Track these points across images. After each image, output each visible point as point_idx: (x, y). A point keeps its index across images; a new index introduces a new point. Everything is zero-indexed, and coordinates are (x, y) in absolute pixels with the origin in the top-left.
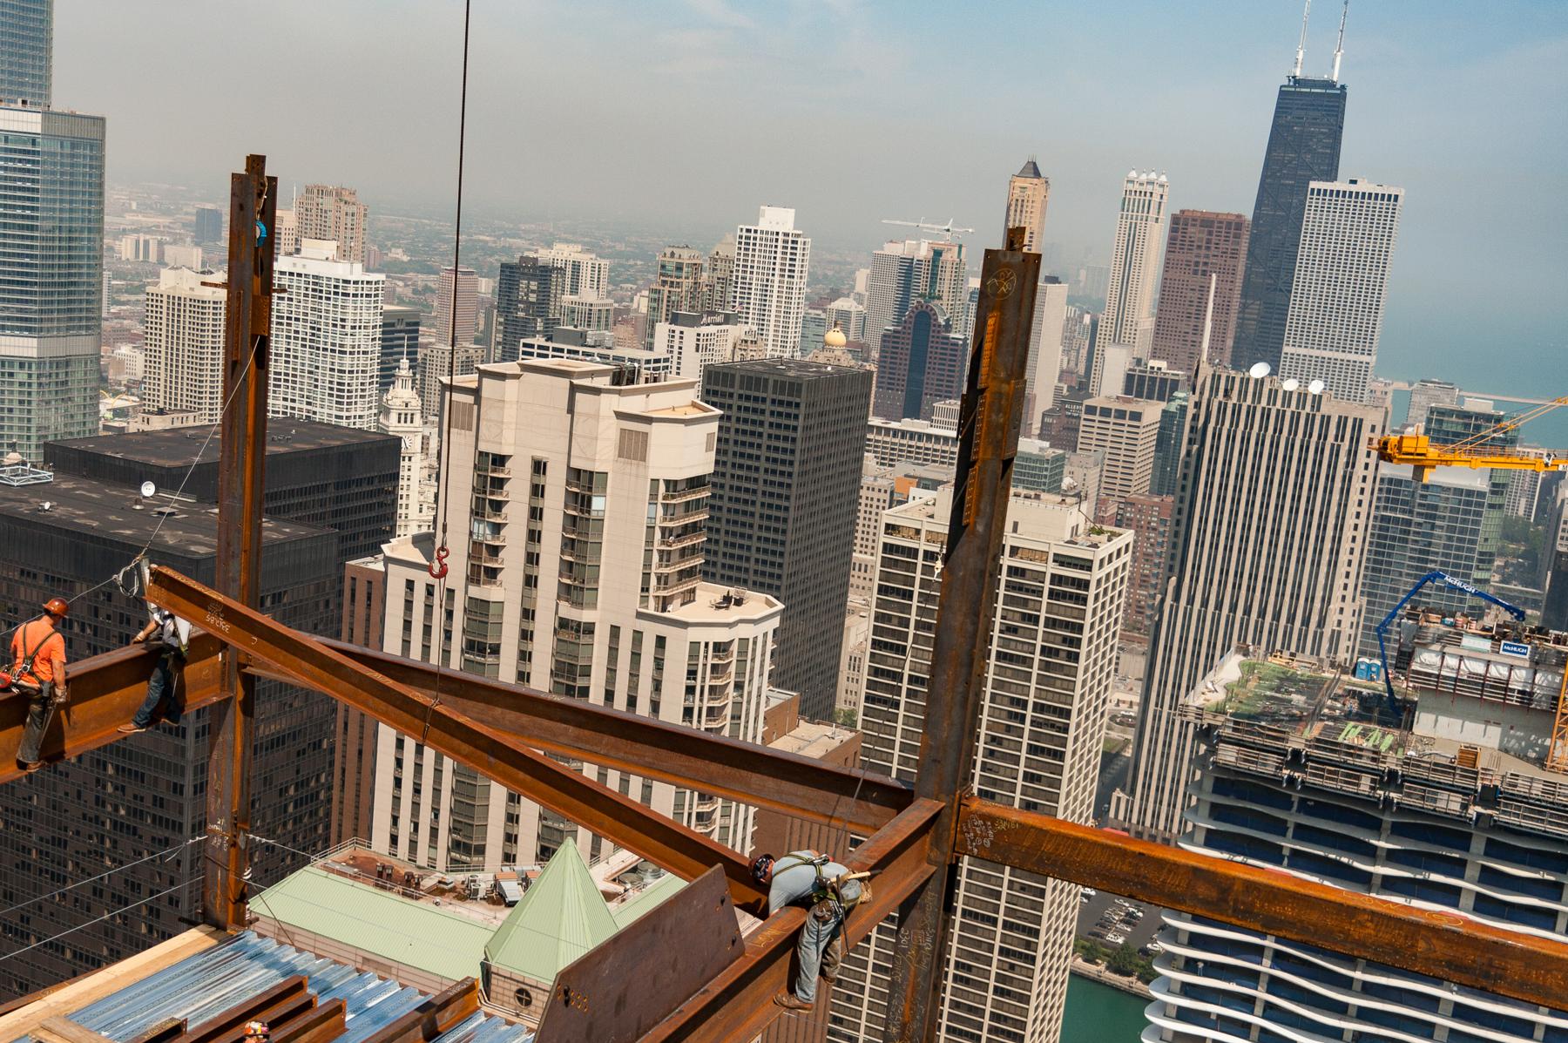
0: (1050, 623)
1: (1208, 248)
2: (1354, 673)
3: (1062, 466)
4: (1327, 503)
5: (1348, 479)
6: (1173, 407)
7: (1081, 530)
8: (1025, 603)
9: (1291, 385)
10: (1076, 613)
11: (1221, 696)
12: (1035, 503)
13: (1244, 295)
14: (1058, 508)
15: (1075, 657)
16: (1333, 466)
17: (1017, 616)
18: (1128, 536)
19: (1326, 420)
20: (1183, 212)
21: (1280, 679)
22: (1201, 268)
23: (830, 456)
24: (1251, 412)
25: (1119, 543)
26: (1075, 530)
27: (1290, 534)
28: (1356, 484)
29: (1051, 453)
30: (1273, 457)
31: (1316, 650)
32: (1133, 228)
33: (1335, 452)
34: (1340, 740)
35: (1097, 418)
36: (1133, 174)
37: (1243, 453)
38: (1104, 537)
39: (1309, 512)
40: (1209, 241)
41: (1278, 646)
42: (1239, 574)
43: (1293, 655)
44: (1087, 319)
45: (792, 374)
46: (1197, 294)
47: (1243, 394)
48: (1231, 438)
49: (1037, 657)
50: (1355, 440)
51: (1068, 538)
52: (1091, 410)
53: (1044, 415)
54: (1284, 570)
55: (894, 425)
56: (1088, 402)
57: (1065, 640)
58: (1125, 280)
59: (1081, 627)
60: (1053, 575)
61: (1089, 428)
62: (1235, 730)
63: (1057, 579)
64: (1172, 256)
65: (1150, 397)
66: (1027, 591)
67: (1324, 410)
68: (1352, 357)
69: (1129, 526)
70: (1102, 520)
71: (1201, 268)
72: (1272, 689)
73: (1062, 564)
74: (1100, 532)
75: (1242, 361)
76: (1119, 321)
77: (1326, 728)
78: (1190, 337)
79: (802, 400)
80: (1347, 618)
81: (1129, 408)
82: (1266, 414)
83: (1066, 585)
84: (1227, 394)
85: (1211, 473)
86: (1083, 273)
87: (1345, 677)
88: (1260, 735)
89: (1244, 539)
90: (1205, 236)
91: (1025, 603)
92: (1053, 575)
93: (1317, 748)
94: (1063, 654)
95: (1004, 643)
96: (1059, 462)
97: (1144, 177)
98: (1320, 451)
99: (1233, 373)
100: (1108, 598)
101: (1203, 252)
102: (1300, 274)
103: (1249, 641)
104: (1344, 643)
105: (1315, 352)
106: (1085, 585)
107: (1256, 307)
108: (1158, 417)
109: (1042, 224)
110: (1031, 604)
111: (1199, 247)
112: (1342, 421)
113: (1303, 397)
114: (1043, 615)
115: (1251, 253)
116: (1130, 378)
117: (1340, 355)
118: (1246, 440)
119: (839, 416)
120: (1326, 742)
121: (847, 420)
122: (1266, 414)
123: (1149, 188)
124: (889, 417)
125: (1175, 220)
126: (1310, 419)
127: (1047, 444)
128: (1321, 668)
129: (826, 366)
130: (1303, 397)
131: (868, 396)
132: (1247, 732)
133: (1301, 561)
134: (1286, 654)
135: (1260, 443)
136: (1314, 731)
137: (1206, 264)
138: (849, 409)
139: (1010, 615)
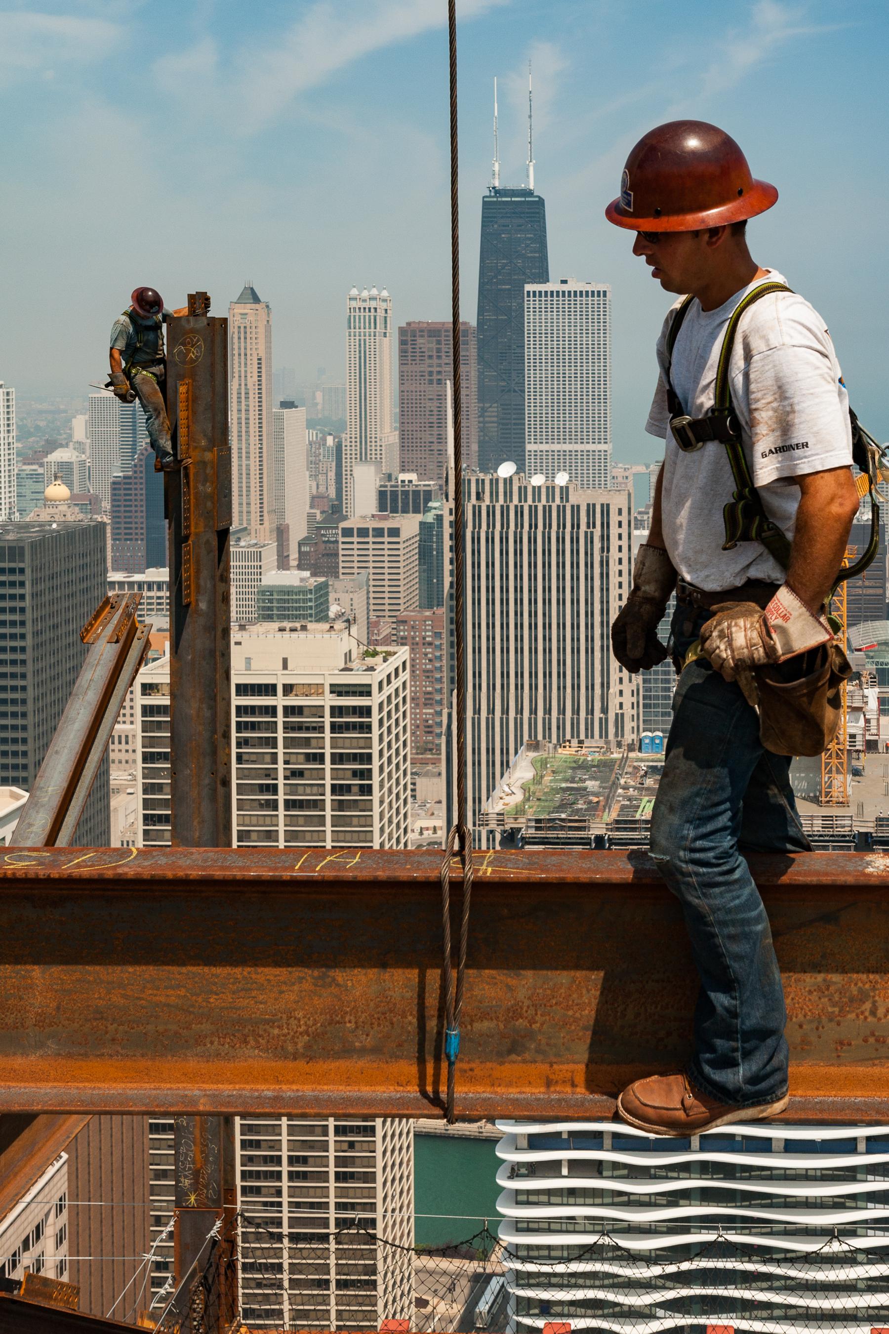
0: (337, 758)
1: (439, 357)
2: (640, 750)
3: (327, 594)
4: (590, 590)
5: (605, 563)
6: (430, 518)
7: (354, 655)
8: (307, 742)
9: (538, 480)
10: (362, 743)
11: (519, 797)
12: (302, 635)
13: (481, 399)
14: (327, 636)
15: (367, 790)
16: (589, 554)
17: (301, 758)
18: (403, 653)
19: (576, 509)
20: (409, 324)
21: (573, 768)
22: (435, 377)
23: (67, 622)
24: (505, 511)
25: (395, 662)
26: (348, 656)
27: (561, 626)
28: (614, 568)
29: (313, 582)
30: (533, 553)
31: (604, 733)
32: (362, 344)
33: (589, 539)
34: (638, 817)
35: (355, 539)
36: (354, 292)
37: (504, 553)
38: (379, 659)
39: (575, 602)
40: (439, 350)
41: (568, 737)
42: (519, 675)
43: (581, 742)
44: (330, 441)
45: (11, 537)
46: (436, 403)
47: (494, 495)
48: (490, 540)
49: (328, 797)
50: (606, 525)
51: (342, 666)
52: (347, 532)
53: (300, 545)
54: (562, 663)
55: (137, 577)
56: (343, 525)
57: (355, 774)
58: (363, 398)
59: (369, 756)
60: (332, 708)
61: (349, 551)
62: (537, 829)
63: (337, 711)
64: (405, 368)
65: (405, 511)
66: (308, 729)
67: (573, 499)
68: (591, 447)
69: (403, 644)
70: (377, 643)
71: (435, 377)
72: (566, 780)
73: (340, 694)
74: (375, 654)
75: (489, 464)
76: (363, 438)
77: (623, 807)
78: (435, 447)
79: (26, 565)
80: (628, 700)
81: (386, 525)
82: (519, 512)
83: (348, 715)
84: (479, 497)
85: (476, 577)
86: (319, 396)
87: (632, 755)
88: (562, 828)
89: (519, 638)
90: (434, 346)
91: (307, 742)
92: (332, 708)
93: (618, 829)
94: (355, 789)
95: (291, 789)
96: (322, 591)
97: (365, 294)
98: (575, 540)
99: (481, 476)
100: (393, 721)
101: (435, 361)
102: (530, 374)
103: (540, 737)
104: (629, 725)
105: (556, 447)
106: (366, 711)
107: (494, 410)
108: (416, 530)
109: (268, 348)
110: (313, 742)
111: (430, 357)
112: (591, 508)
113: (551, 490)
114: (328, 751)
115: (481, 359)
116: (382, 495)
117: (579, 447)
118: (504, 539)
119: (73, 576)
120: (626, 822)
121: (82, 580)
122: (519, 512)
123: (373, 304)
124: (130, 570)
125: (402, 331)
126: (561, 510)
127: (307, 574)
128: (609, 749)
129: (50, 523)
130: (551, 490)
131: (103, 550)
132: (549, 829)
133: (575, 651)
134: (575, 742)
135: (518, 540)
136: (612, 815)
137: (439, 372)
138: (83, 567)
139: (293, 759)
